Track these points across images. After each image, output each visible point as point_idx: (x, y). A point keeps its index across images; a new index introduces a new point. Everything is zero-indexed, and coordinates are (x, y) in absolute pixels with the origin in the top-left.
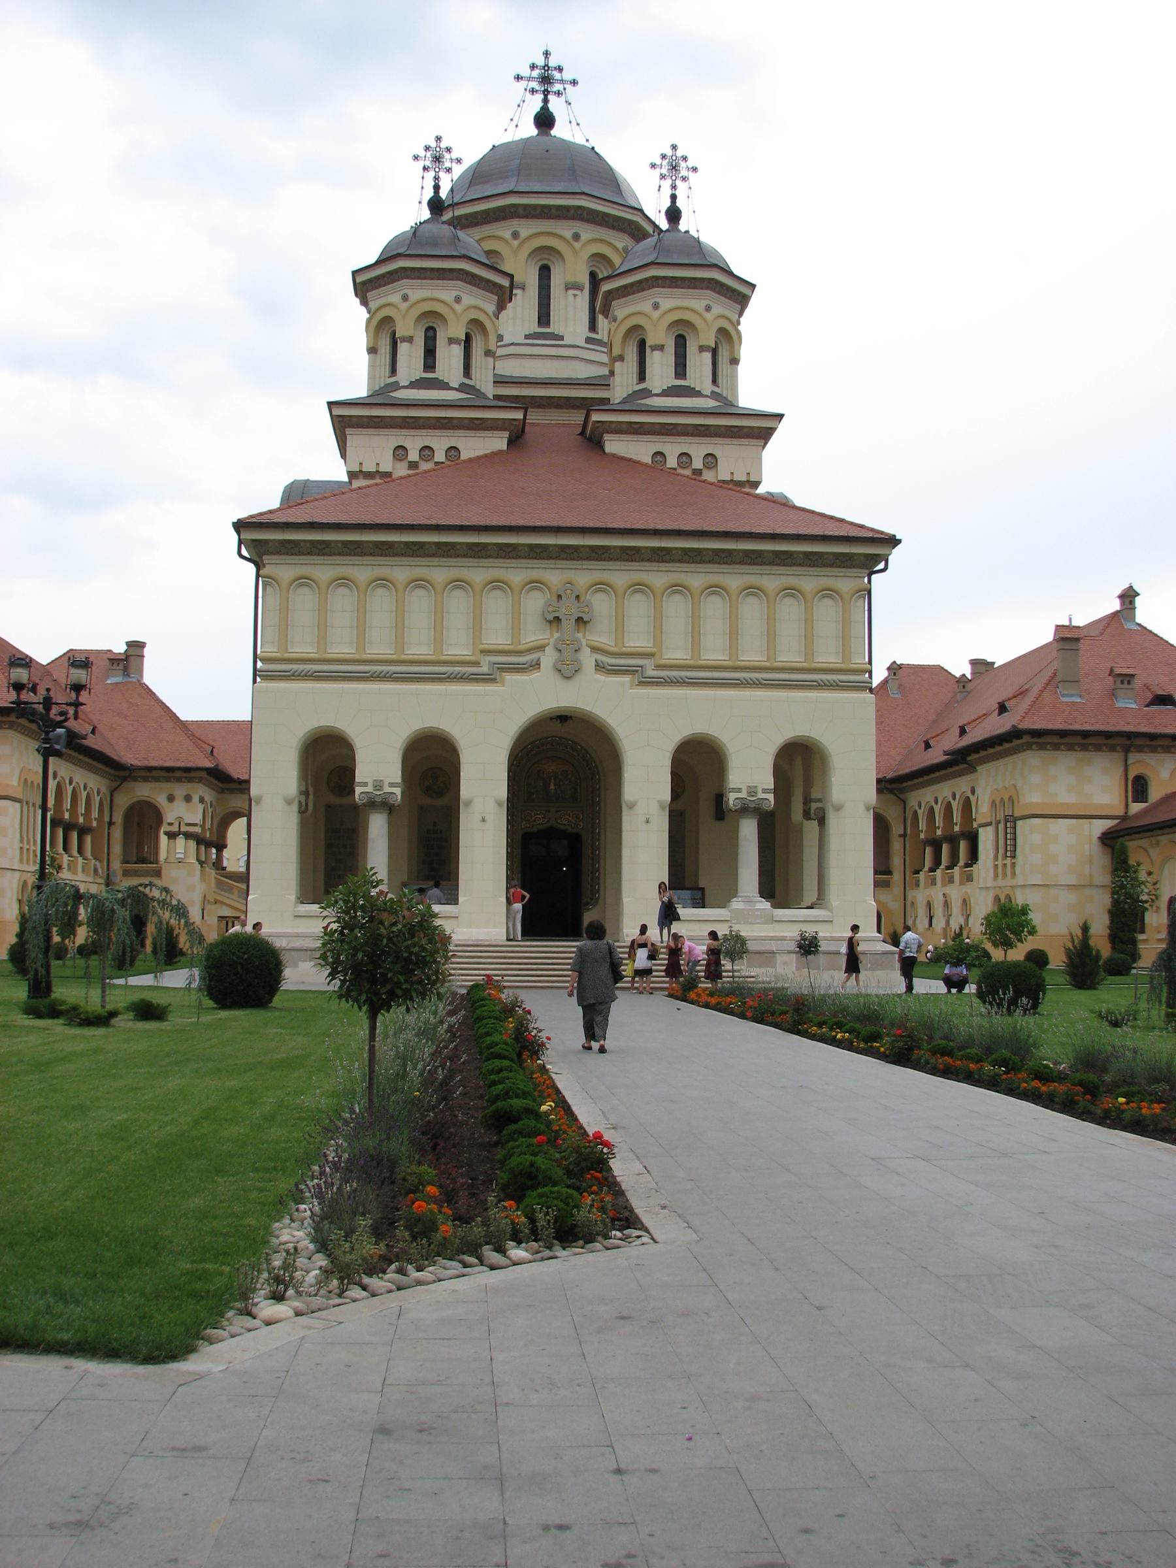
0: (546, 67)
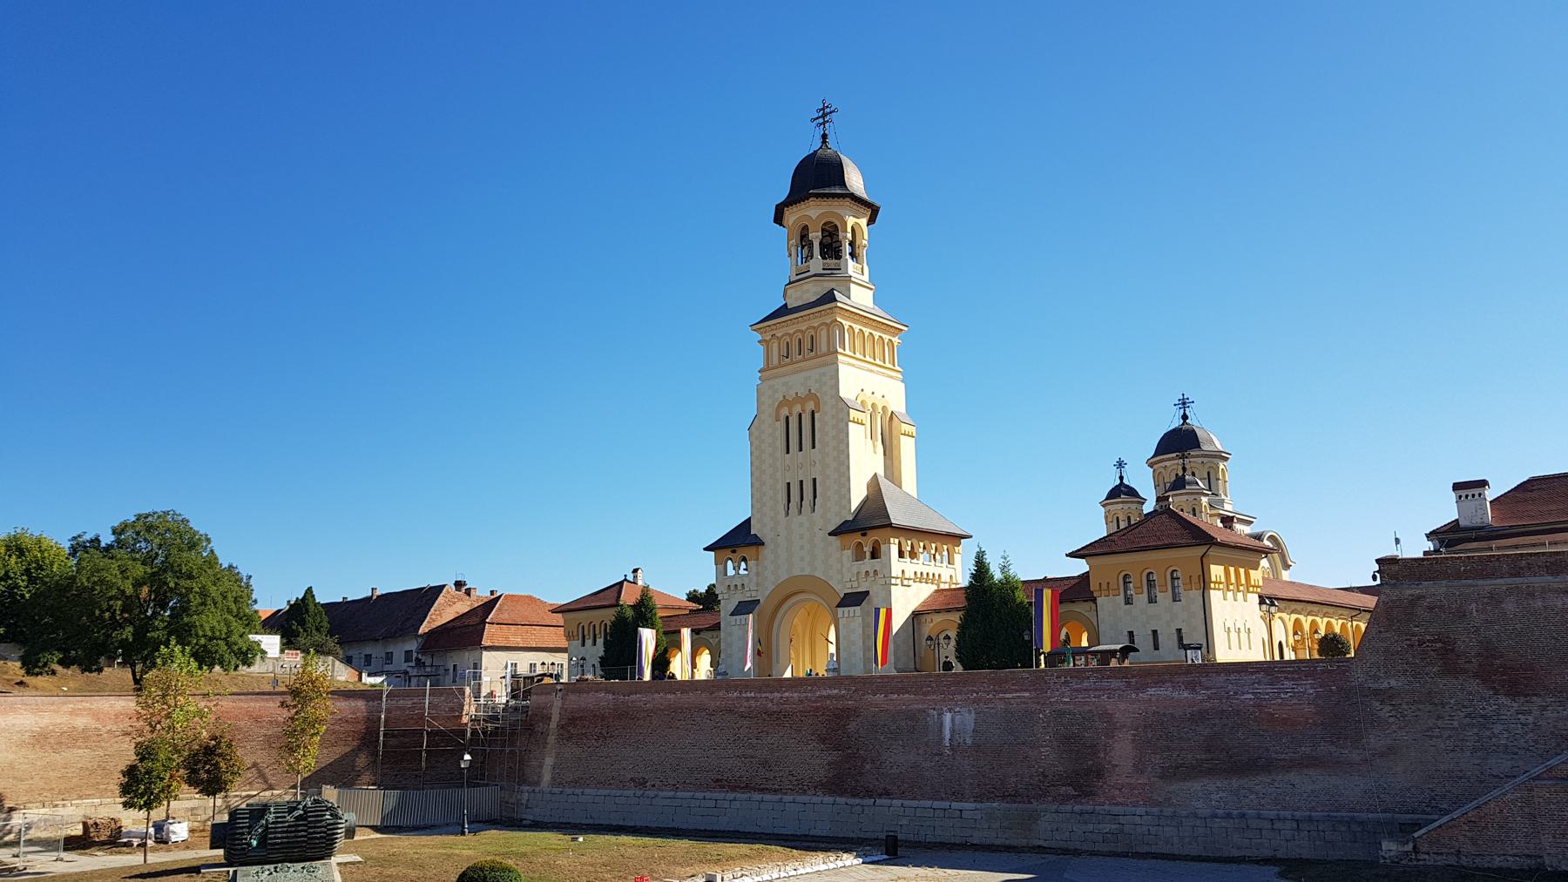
0: (1183, 399)
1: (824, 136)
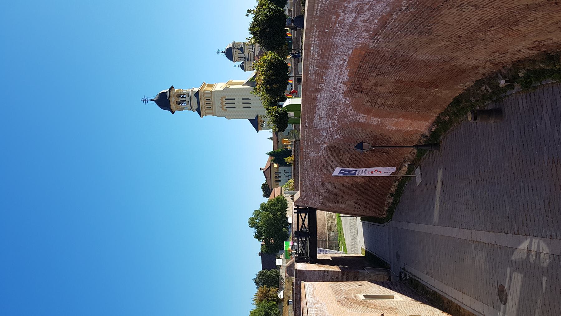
1: (151, 100)
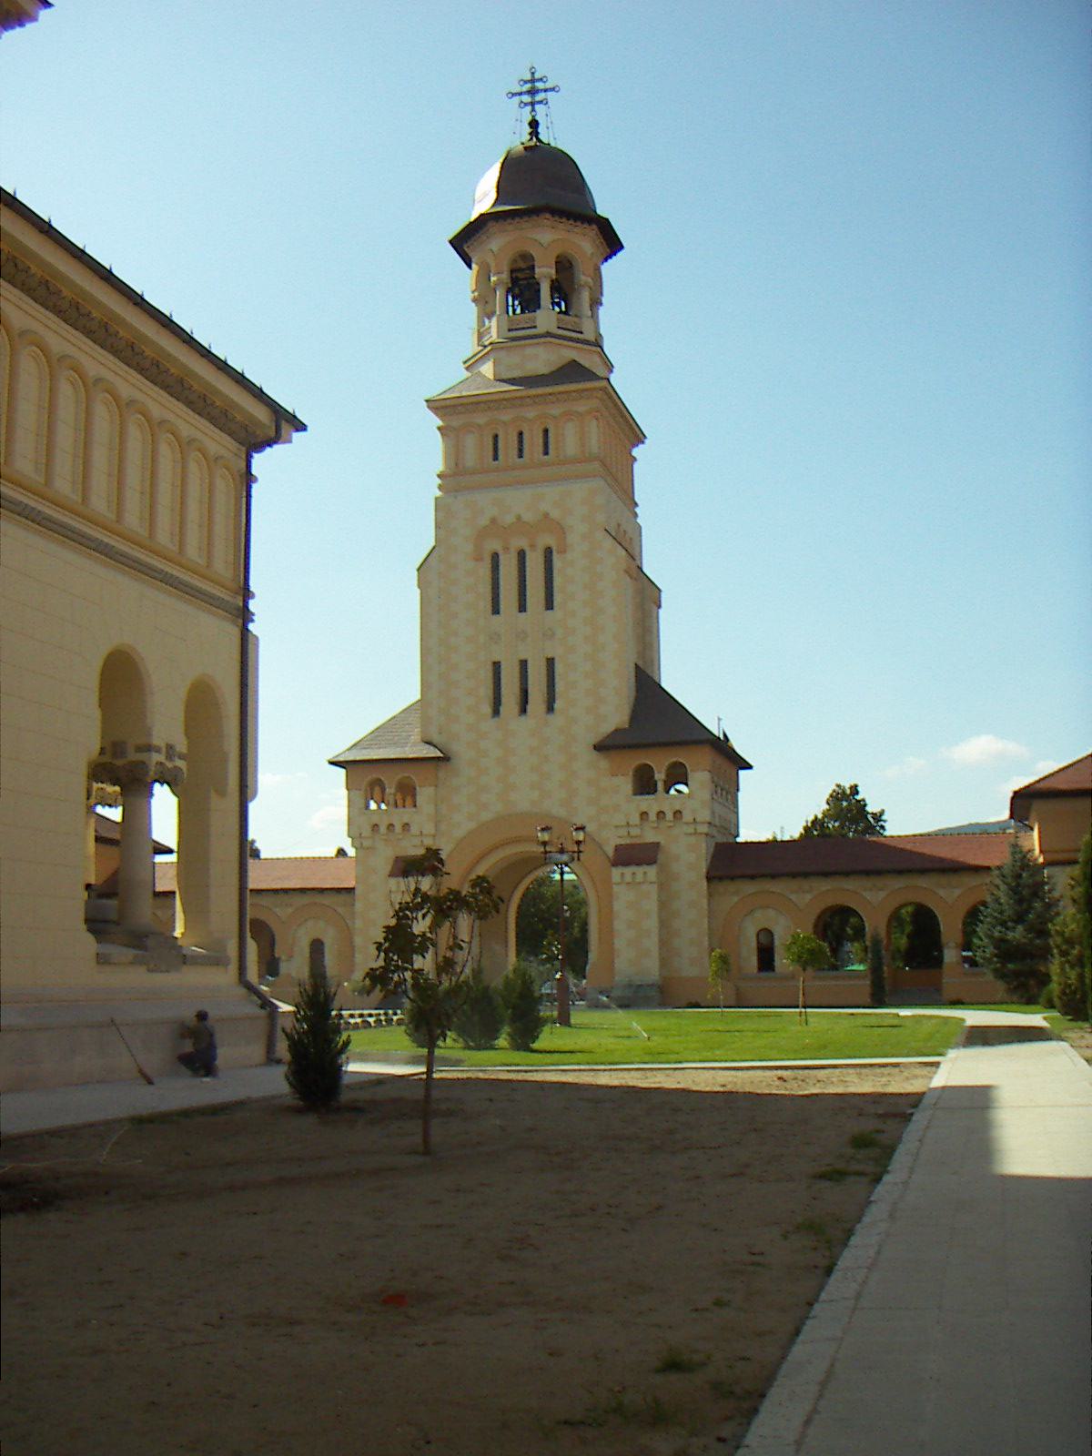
1: (534, 124)
